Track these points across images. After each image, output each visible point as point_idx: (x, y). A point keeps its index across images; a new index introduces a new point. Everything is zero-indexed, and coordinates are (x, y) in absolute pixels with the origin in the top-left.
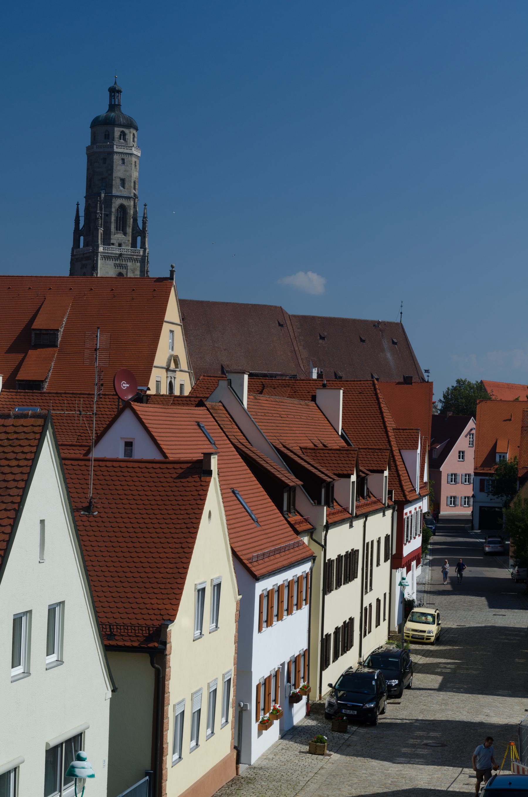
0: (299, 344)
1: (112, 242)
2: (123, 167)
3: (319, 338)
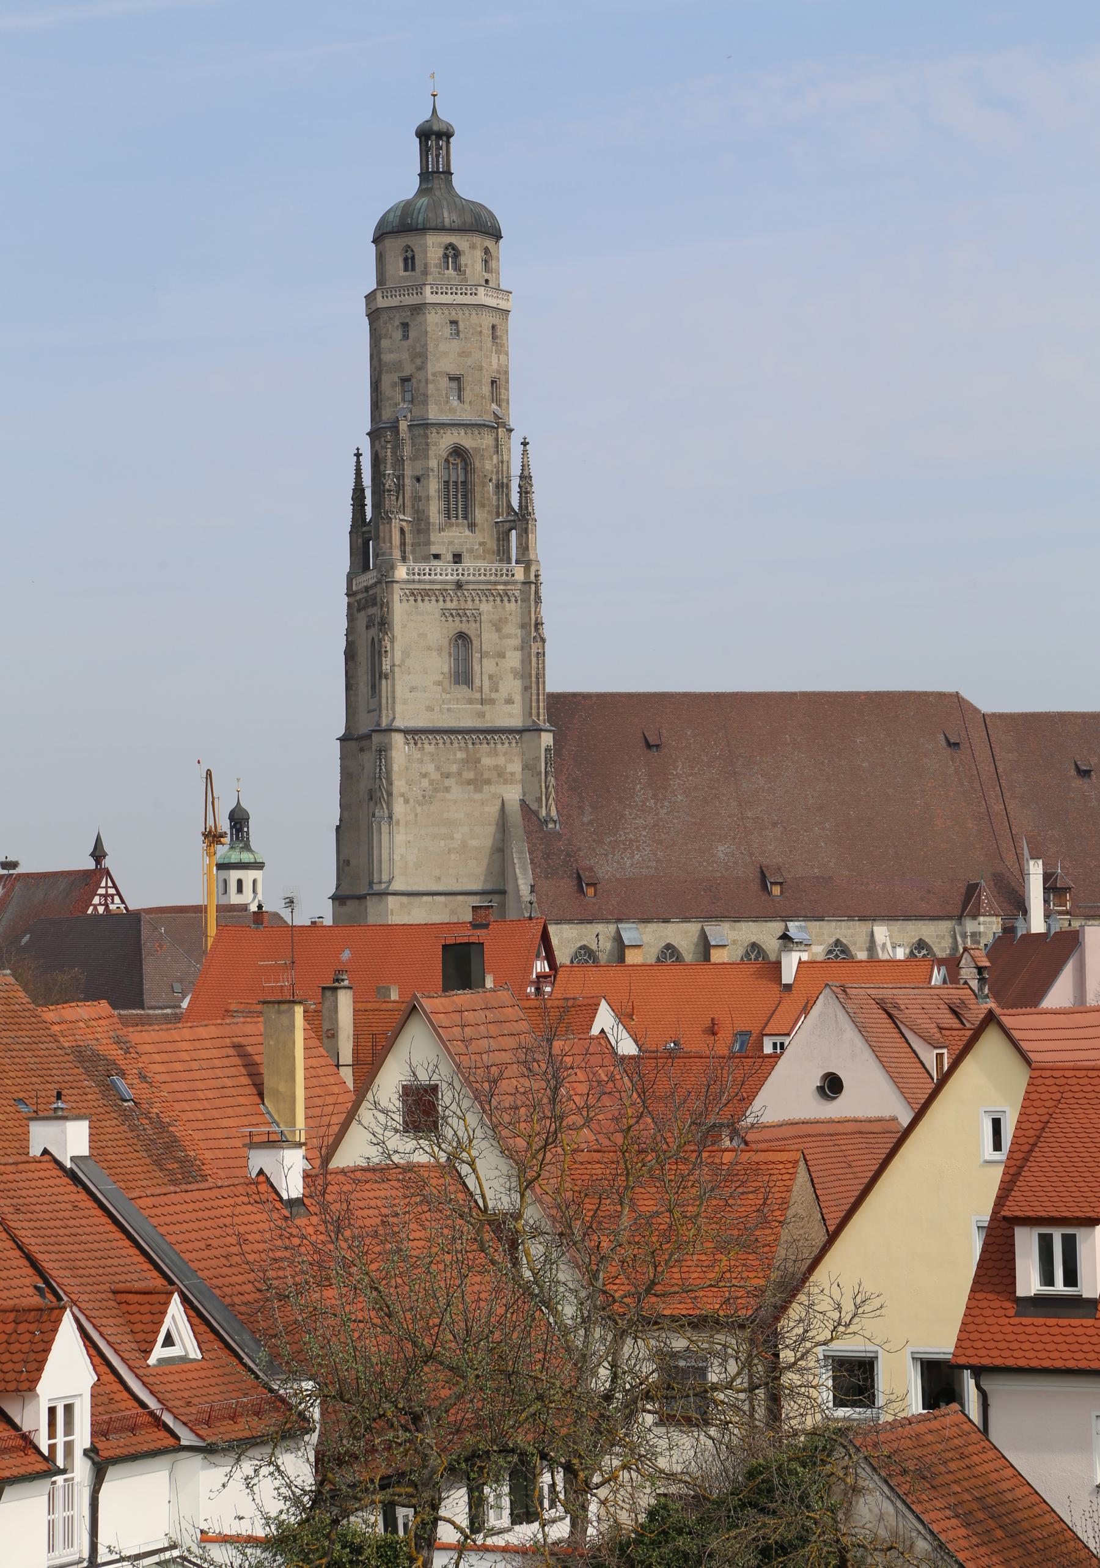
0: (1007, 794)
1: (433, 551)
2: (455, 345)
3: (1073, 772)
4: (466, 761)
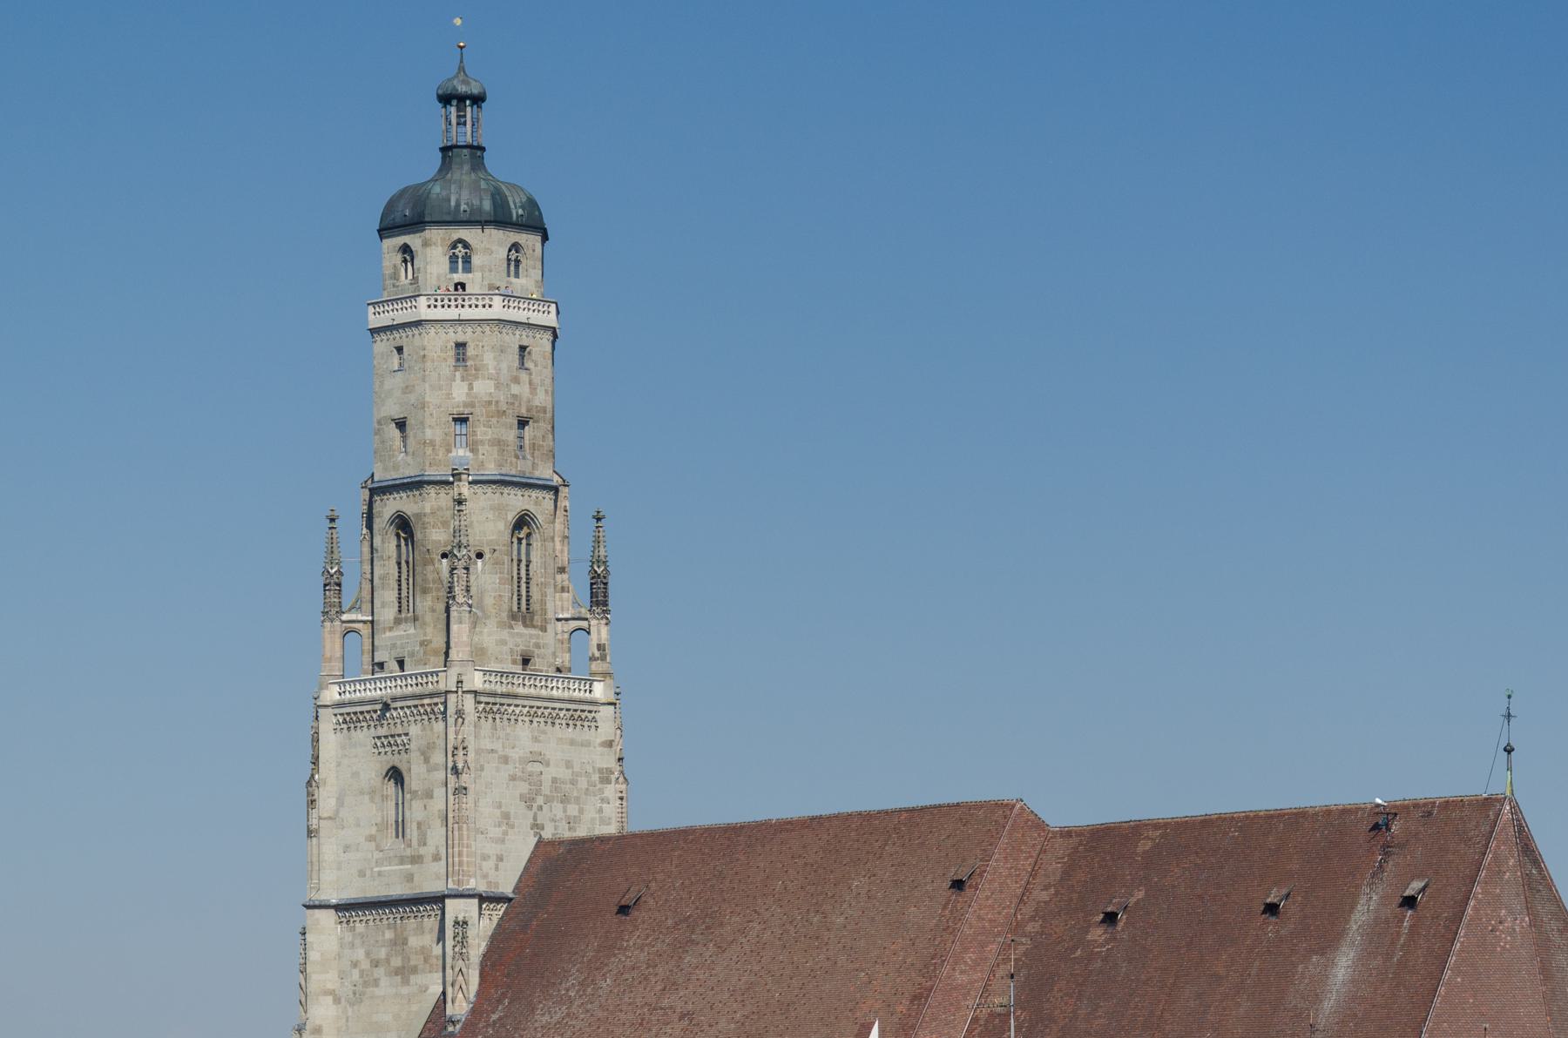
4: (394, 943)
